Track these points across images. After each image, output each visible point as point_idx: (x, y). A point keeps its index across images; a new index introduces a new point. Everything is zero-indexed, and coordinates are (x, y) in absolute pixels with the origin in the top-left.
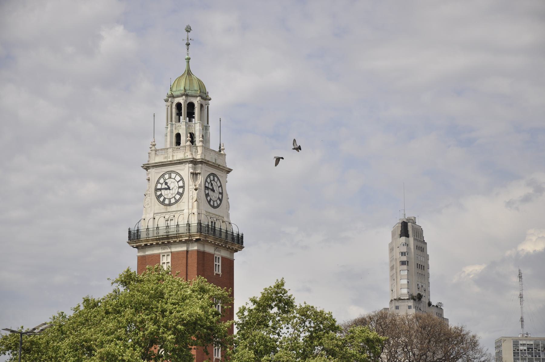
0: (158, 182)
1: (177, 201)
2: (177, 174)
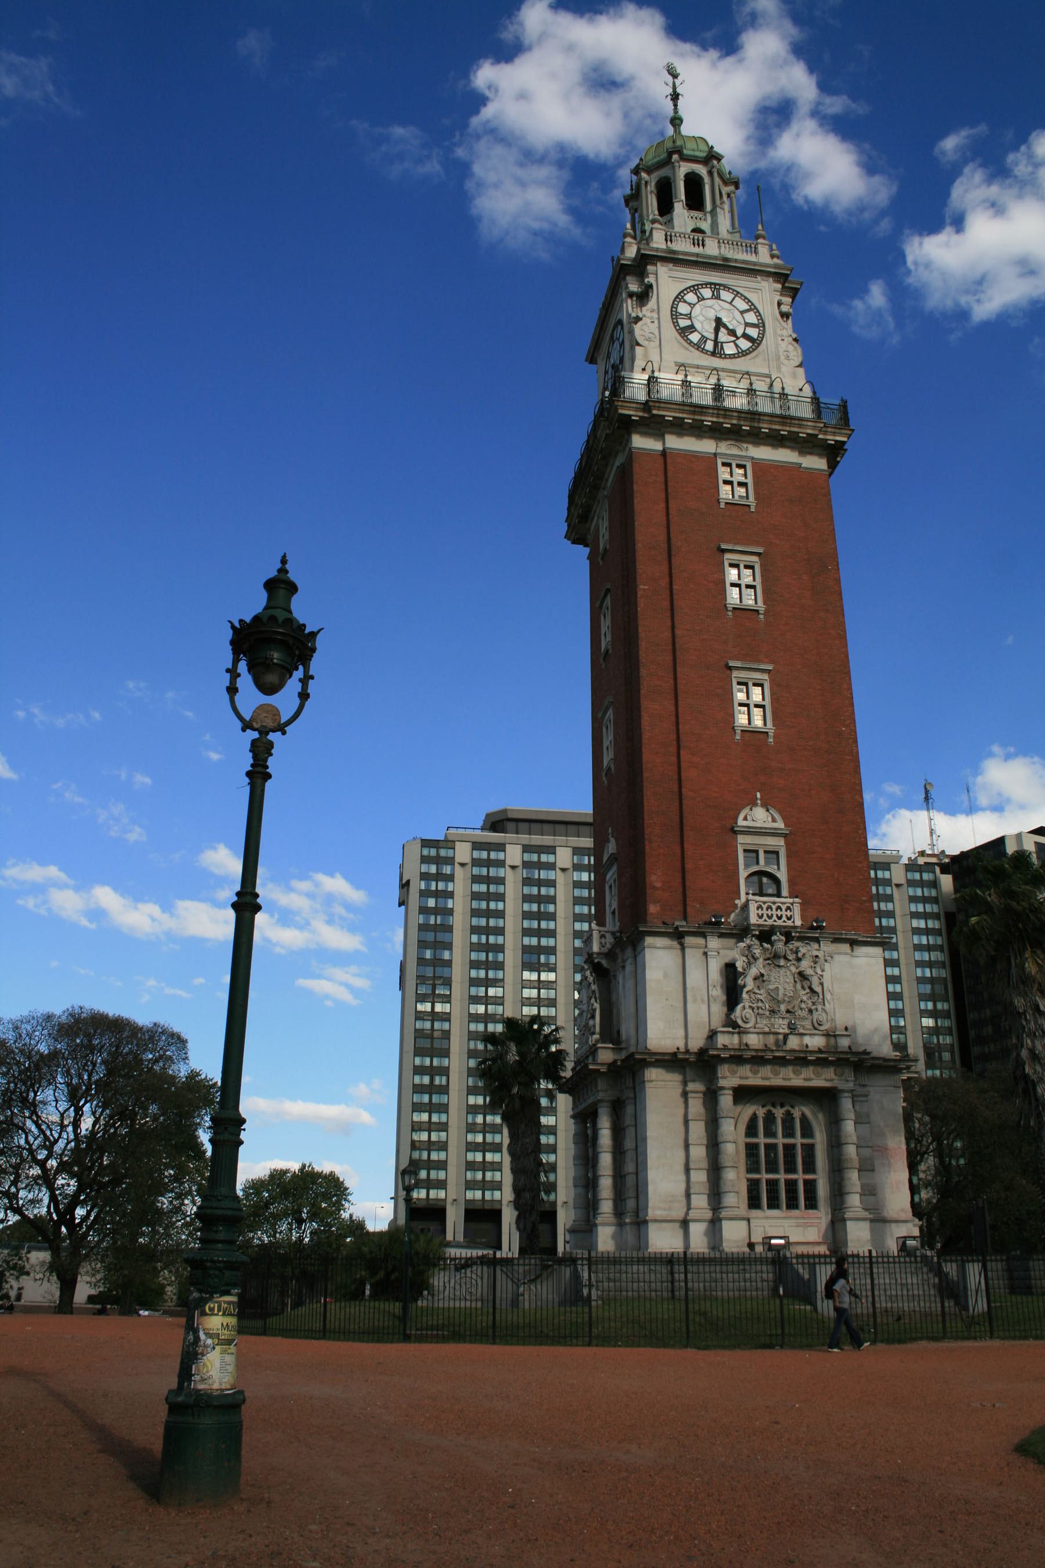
0: (679, 298)
1: (743, 354)
2: (737, 294)
